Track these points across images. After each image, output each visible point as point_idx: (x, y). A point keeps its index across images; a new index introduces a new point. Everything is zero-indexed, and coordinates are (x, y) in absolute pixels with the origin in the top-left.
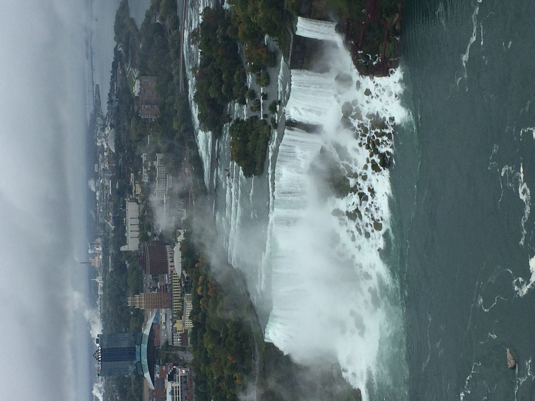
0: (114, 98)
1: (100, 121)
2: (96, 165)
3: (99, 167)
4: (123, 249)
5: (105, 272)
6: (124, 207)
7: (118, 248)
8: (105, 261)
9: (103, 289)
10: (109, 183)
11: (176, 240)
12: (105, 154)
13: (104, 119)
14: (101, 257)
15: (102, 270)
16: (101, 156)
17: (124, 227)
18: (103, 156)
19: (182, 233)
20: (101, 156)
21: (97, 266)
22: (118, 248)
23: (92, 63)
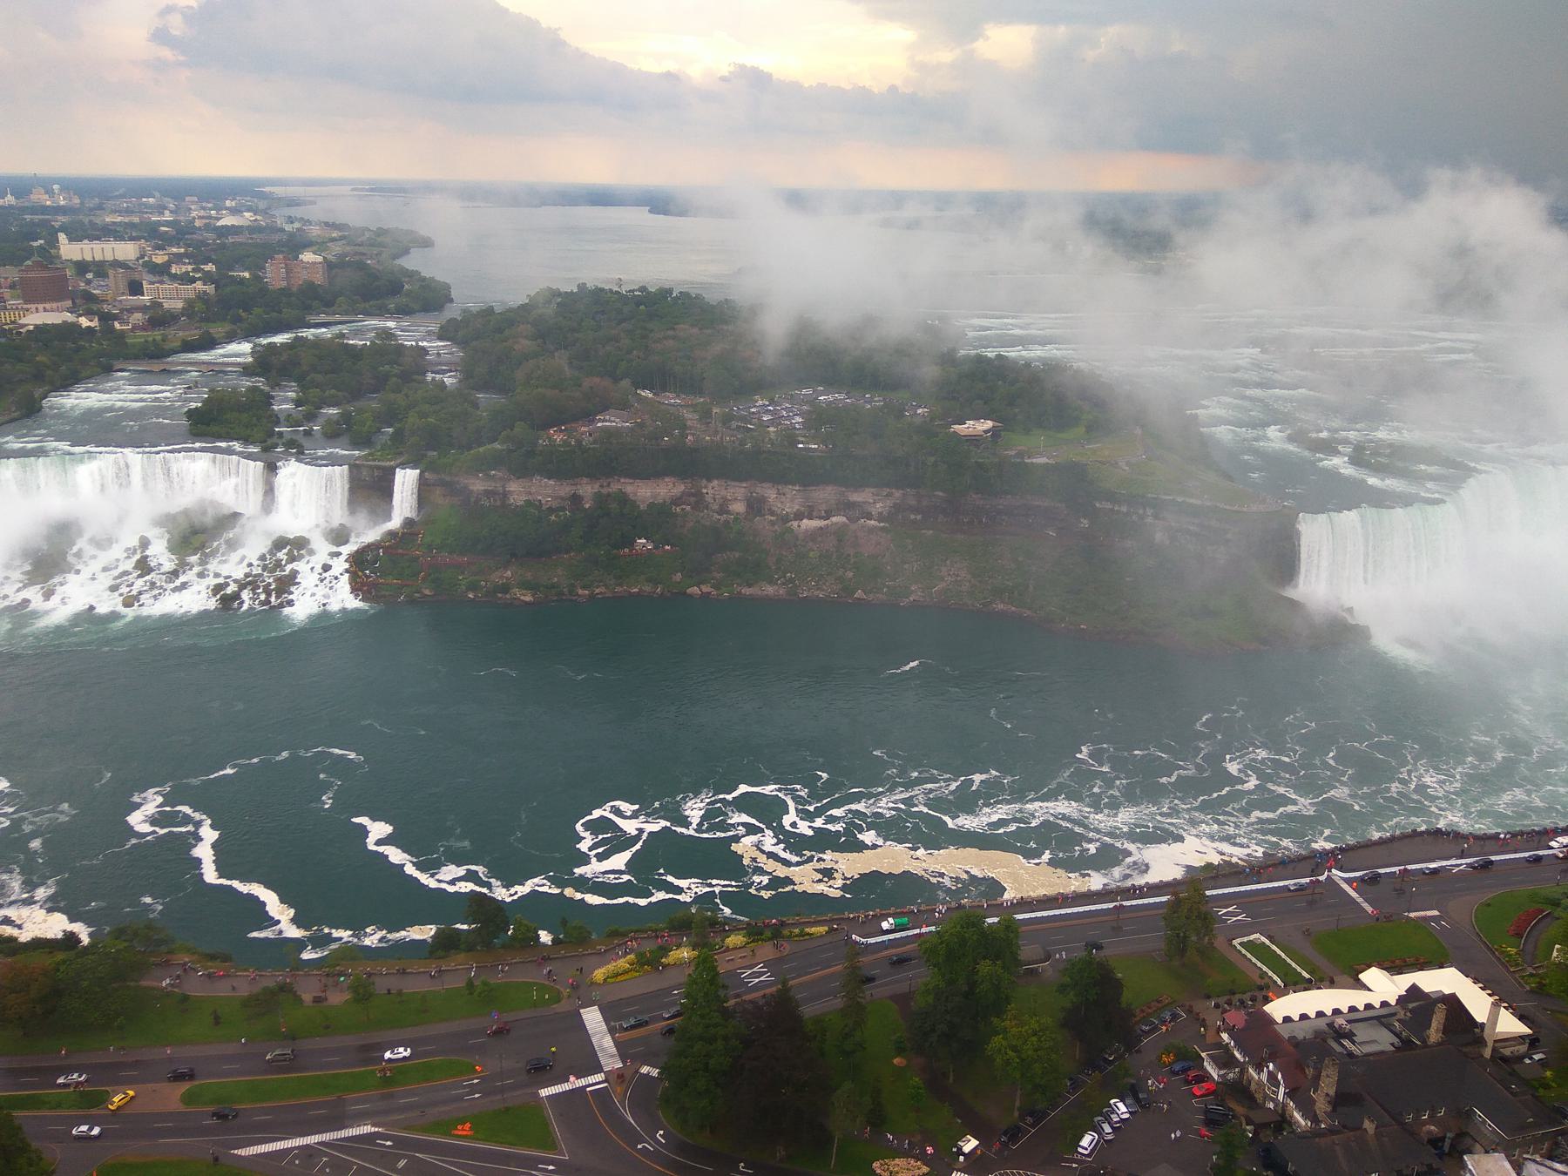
0: (297, 225)
1: (262, 205)
2: (196, 199)
3: (193, 203)
4: (62, 237)
5: (23, 210)
6: (132, 239)
7: (63, 229)
8: (44, 210)
10: (168, 217)
11: (81, 315)
13: (265, 212)
14: (48, 203)
15: (26, 204)
16: (210, 205)
19: (92, 324)
20: (210, 205)
21: (32, 196)
22: (63, 229)
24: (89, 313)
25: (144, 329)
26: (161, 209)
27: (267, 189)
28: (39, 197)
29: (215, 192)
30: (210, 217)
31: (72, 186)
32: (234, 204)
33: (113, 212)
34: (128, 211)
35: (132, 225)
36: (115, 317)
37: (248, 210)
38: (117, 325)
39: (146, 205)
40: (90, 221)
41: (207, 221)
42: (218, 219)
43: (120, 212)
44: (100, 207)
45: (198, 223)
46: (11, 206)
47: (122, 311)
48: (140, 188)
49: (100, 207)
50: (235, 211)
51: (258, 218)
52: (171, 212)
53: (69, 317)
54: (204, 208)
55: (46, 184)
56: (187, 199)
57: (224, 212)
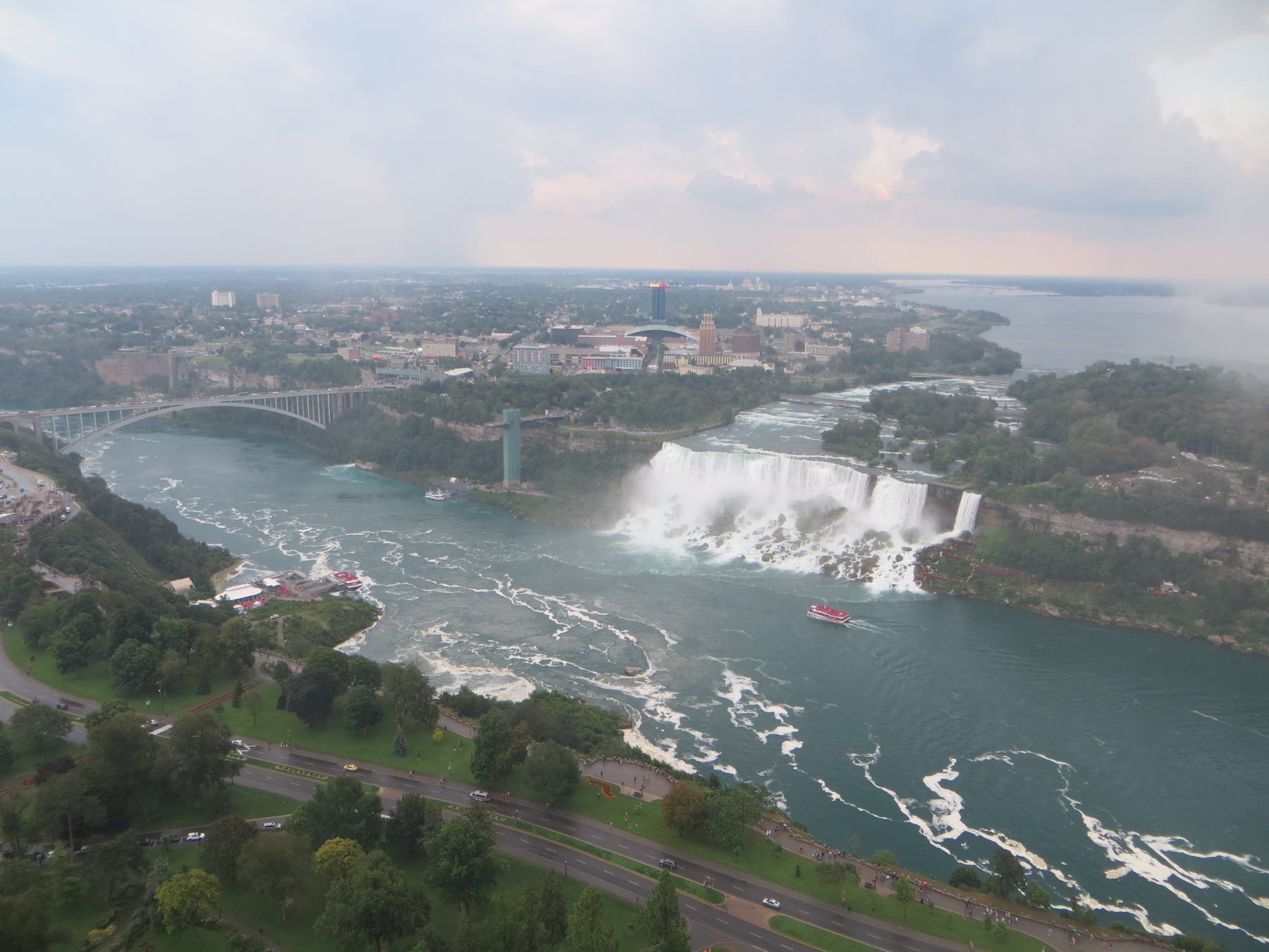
0: (909, 307)
2: (842, 288)
3: (840, 290)
4: (759, 311)
5: (739, 293)
6: (799, 313)
7: (760, 305)
8: (749, 293)
9: (721, 290)
10: (823, 299)
11: (764, 363)
12: (853, 297)
14: (752, 289)
16: (851, 292)
17: (779, 312)
20: (851, 292)
21: (744, 285)
22: (760, 305)
24: (769, 361)
26: (819, 294)
27: (890, 281)
28: (747, 285)
29: (854, 284)
30: (851, 300)
31: (767, 279)
32: (867, 292)
33: (790, 295)
34: (799, 295)
35: (799, 304)
36: (784, 365)
37: (877, 295)
38: (785, 370)
39: (811, 291)
40: (776, 301)
41: (848, 303)
42: (856, 302)
43: (794, 295)
44: (782, 292)
45: (842, 304)
46: (731, 290)
47: (789, 361)
48: (806, 280)
49: (782, 292)
50: (868, 296)
51: (884, 301)
52: (826, 296)
53: (757, 363)
54: (846, 294)
55: (752, 277)
56: (837, 287)
57: (860, 297)
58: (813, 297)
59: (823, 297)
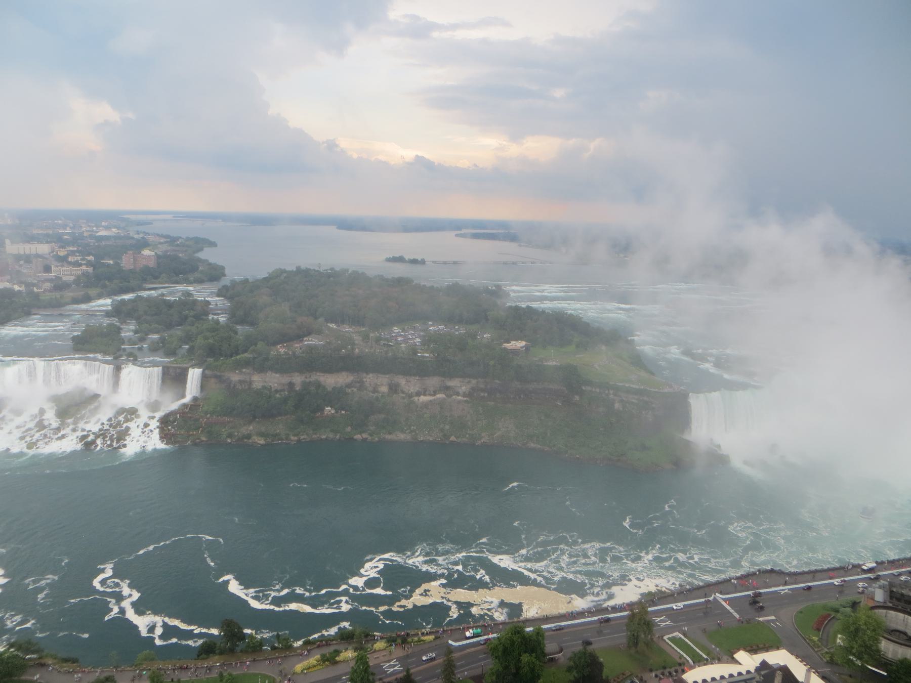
0: (141, 235)
2: (85, 221)
6: (47, 242)
10: (68, 230)
11: (14, 284)
12: (94, 228)
16: (93, 225)
18: (93, 227)
19: (21, 289)
23: (510, 254)
24: (20, 283)
25: (50, 291)
26: (65, 226)
30: (93, 231)
32: (106, 224)
35: (47, 235)
37: (115, 227)
38: (35, 290)
42: (97, 232)
45: (85, 234)
50: (107, 228)
51: (120, 231)
52: (71, 228)
53: (7, 285)
54: (89, 226)
58: (59, 229)
59: (68, 228)
